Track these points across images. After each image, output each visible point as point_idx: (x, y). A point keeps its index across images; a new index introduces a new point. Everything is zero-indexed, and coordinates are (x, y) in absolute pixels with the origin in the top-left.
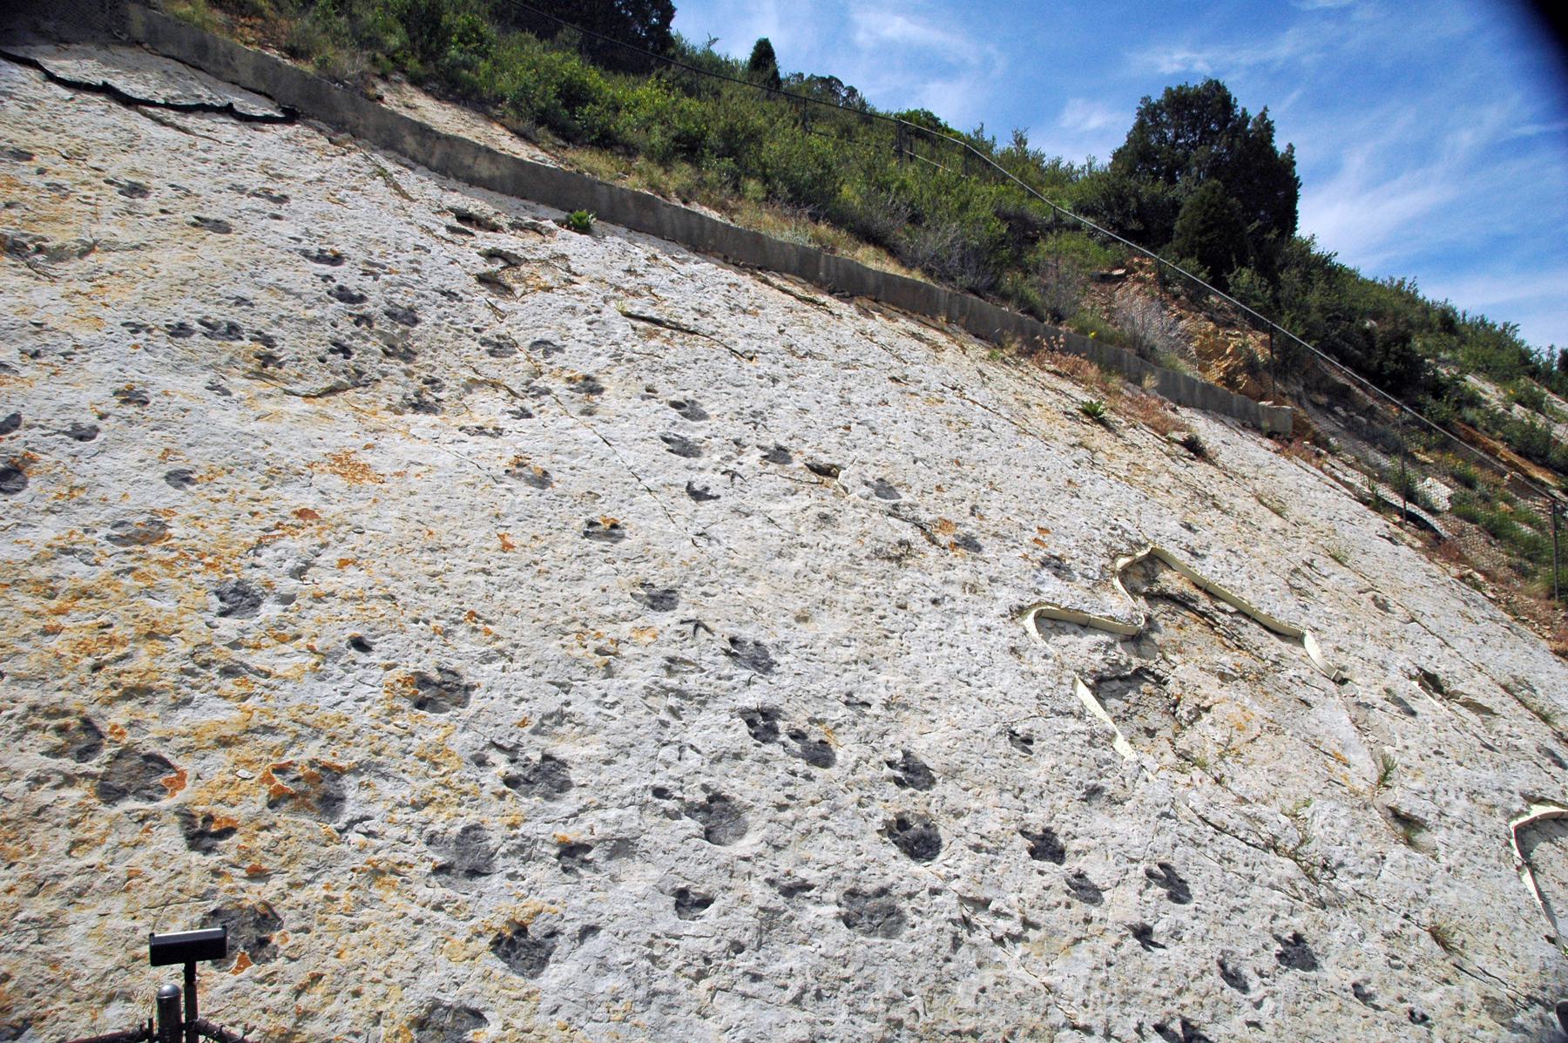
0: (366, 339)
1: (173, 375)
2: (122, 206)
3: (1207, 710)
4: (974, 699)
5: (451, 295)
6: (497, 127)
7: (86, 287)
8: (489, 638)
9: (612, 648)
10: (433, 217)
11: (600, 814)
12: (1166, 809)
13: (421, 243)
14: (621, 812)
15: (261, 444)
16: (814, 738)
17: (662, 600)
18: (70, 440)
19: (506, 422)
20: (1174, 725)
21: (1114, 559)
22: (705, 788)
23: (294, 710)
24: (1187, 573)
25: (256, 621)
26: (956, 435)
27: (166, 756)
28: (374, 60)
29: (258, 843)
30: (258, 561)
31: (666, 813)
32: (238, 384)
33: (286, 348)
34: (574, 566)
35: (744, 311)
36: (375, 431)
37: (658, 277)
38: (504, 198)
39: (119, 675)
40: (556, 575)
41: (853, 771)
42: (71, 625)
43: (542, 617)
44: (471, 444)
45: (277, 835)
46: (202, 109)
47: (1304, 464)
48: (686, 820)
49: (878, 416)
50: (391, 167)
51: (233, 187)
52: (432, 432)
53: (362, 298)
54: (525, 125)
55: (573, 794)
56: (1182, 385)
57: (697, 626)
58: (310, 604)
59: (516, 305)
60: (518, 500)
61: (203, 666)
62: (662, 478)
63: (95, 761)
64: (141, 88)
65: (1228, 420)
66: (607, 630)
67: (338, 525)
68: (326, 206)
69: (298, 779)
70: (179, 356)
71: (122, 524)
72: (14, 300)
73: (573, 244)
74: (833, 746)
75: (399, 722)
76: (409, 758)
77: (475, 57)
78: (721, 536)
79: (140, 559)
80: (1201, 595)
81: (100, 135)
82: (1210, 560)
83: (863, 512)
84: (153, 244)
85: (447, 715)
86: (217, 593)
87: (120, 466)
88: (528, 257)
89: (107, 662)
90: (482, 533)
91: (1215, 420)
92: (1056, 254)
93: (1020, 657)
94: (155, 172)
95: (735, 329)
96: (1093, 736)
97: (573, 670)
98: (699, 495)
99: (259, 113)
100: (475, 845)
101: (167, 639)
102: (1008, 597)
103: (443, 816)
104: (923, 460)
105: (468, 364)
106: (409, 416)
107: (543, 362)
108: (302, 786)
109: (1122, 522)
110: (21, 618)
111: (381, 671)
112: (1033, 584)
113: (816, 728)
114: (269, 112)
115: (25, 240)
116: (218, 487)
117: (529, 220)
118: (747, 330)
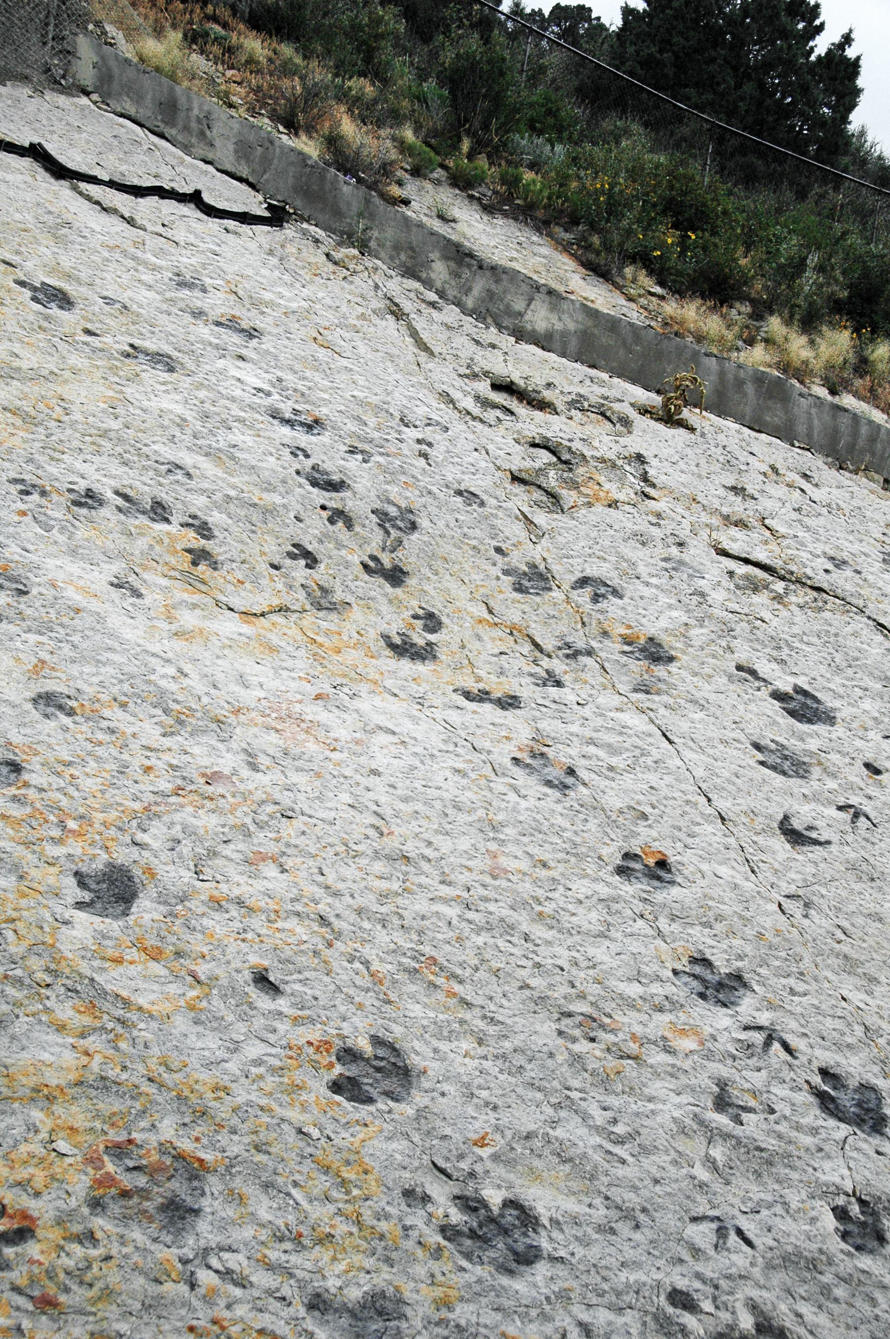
5: (469, 496)
9: (633, 1048)
10: (459, 382)
14: (611, 1316)
15: (171, 671)
22: (753, 1307)
30: (140, 837)
43: (533, 982)
55: (542, 1269)
86: (76, 874)
90: (464, 844)
108: (142, 1181)
116: (104, 724)
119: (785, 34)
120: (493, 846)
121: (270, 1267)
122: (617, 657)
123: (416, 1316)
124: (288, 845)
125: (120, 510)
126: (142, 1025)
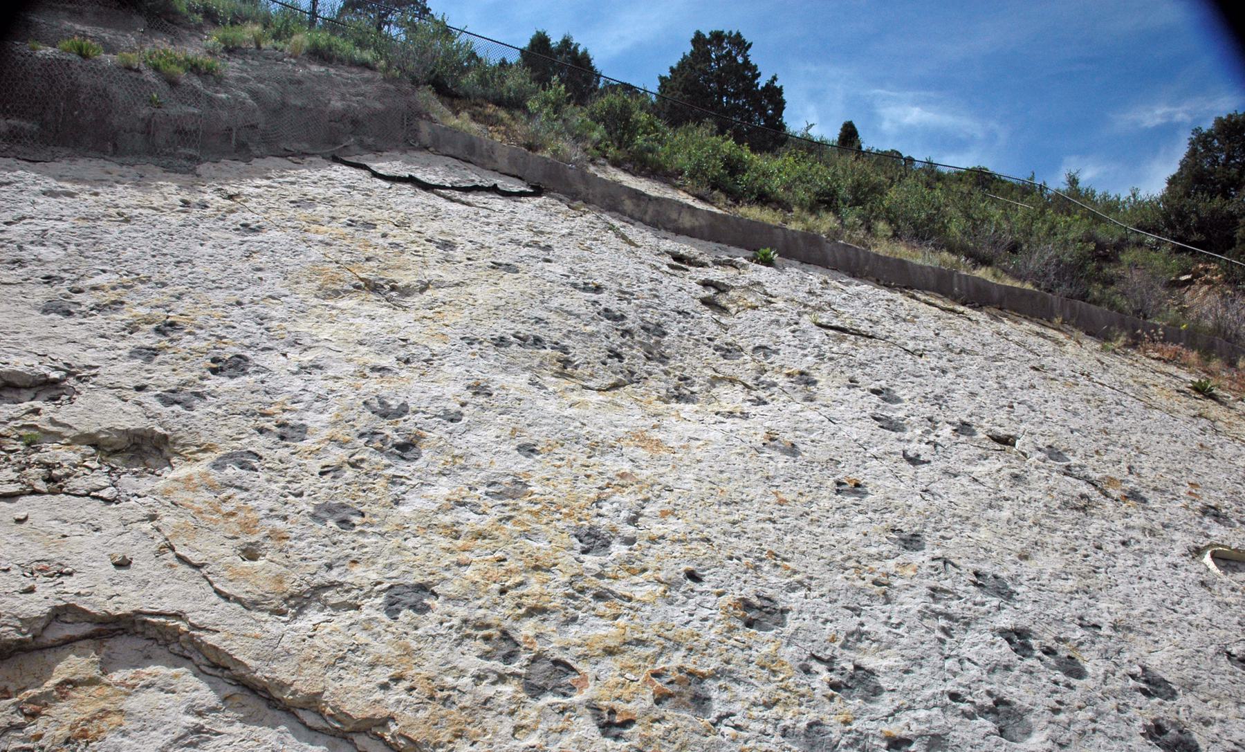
0: (631, 348)
1: (504, 375)
2: (441, 256)
6: (681, 193)
7: (430, 314)
8: (788, 572)
9: (884, 579)
10: (658, 258)
11: (912, 714)
13: (654, 276)
14: (928, 712)
15: (578, 424)
16: (1065, 655)
17: (912, 542)
18: (445, 422)
19: (747, 407)
22: (989, 693)
25: (610, 558)
26: (1096, 411)
27: (569, 661)
28: (585, 150)
29: (654, 733)
30: (601, 511)
31: (964, 714)
32: (549, 380)
33: (577, 355)
34: (837, 516)
35: (904, 320)
36: (655, 415)
37: (832, 296)
38: (703, 242)
39: (520, 597)
40: (826, 523)
41: (1105, 682)
42: (477, 559)
43: (824, 555)
44: (729, 424)
46: (476, 189)
48: (982, 720)
49: (1033, 397)
50: (617, 224)
51: (512, 241)
53: (623, 317)
54: (703, 190)
55: (886, 697)
57: (945, 563)
58: (648, 545)
59: (735, 320)
60: (780, 465)
61: (580, 592)
63: (517, 664)
64: (434, 177)
66: (875, 565)
67: (652, 485)
68: (578, 252)
69: (671, 682)
70: (505, 360)
71: (494, 483)
73: (764, 274)
75: (739, 638)
76: (753, 667)
77: (656, 144)
78: (941, 492)
79: (514, 510)
81: (415, 210)
83: (1045, 473)
84: (468, 281)
85: (773, 632)
88: (734, 285)
89: (509, 587)
90: (761, 491)
94: (457, 232)
95: (903, 332)
98: (915, 461)
99: (516, 190)
100: (819, 738)
101: (548, 571)
103: (790, 714)
104: (1078, 430)
105: (708, 365)
106: (674, 405)
107: (765, 362)
108: (676, 688)
110: (441, 553)
111: (715, 598)
113: (1062, 646)
114: (523, 189)
115: (382, 282)
116: (557, 456)
117: (726, 258)
118: (911, 334)
119: (745, 78)
120: (774, 489)
121: (756, 720)
122: (790, 384)
124: (676, 505)
126: (643, 609)
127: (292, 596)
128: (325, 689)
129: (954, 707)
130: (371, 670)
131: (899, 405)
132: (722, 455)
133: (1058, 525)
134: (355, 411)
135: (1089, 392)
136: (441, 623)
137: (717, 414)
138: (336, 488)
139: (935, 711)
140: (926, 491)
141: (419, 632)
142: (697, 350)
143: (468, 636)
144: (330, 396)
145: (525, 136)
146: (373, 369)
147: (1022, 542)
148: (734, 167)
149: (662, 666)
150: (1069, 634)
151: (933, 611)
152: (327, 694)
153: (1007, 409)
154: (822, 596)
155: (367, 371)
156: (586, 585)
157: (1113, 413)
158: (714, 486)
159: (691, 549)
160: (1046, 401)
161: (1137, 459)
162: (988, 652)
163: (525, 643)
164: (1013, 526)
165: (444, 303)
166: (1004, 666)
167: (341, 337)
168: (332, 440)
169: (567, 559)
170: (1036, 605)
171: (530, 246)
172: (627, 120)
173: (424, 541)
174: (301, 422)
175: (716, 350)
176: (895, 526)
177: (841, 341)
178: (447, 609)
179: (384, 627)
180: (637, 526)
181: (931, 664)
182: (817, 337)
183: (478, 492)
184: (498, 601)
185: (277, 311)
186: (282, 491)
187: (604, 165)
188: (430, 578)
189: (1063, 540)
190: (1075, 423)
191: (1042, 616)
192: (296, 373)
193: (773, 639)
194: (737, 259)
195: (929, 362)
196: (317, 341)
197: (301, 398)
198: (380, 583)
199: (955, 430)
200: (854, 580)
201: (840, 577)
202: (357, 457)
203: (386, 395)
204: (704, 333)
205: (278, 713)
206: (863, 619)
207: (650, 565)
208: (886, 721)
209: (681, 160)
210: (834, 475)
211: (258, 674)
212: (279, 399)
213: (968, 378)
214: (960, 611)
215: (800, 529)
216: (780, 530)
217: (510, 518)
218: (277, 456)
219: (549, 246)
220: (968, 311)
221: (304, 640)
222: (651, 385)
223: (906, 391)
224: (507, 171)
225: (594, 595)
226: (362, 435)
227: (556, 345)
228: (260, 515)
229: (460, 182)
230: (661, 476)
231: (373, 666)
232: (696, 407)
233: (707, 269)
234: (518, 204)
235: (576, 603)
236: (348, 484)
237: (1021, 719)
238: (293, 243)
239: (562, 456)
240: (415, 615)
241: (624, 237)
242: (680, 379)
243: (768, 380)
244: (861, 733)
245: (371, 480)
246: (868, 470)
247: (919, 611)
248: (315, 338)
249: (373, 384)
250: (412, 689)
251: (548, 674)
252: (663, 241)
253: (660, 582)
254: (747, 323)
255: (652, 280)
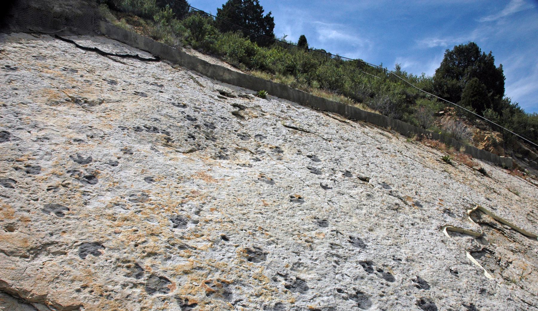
0: (199, 133)
1: (139, 144)
2: (110, 88)
3: (511, 263)
4: (435, 258)
6: (225, 63)
7: (103, 115)
8: (268, 236)
9: (310, 240)
11: (321, 298)
12: (509, 297)
13: (211, 101)
14: (328, 298)
15: (173, 168)
16: (386, 272)
17: (323, 223)
19: (251, 162)
20: (500, 268)
21: (466, 210)
22: (354, 289)
23: (207, 261)
24: (491, 215)
26: (403, 167)
27: (167, 277)
28: (181, 41)
30: (183, 208)
31: (343, 298)
32: (160, 148)
33: (174, 136)
34: (290, 211)
35: (323, 125)
36: (209, 165)
37: (292, 113)
38: (234, 86)
39: (144, 248)
40: (285, 214)
42: (124, 230)
43: (284, 229)
44: (243, 169)
45: (212, 306)
47: (519, 178)
48: (351, 300)
49: (377, 161)
50: (195, 76)
51: (144, 82)
52: (229, 166)
53: (196, 119)
54: (235, 63)
55: (310, 291)
56: (473, 151)
57: (337, 232)
58: (204, 224)
59: (247, 122)
60: (265, 189)
61: (172, 245)
62: (311, 182)
63: (142, 279)
64: (107, 49)
65: (489, 163)
66: (306, 233)
67: (207, 197)
68: (176, 88)
69: (214, 286)
70: (139, 138)
71: (133, 195)
72: (79, 119)
73: (261, 102)
74: (393, 274)
75: (245, 266)
76: (251, 279)
77: (214, 40)
78: (336, 202)
79: (142, 207)
80: (498, 223)
81: (97, 65)
82: (498, 211)
84: (123, 100)
85: (260, 263)
86: (171, 220)
87: (128, 175)
89: (139, 243)
91: (486, 163)
92: (421, 106)
93: (445, 244)
94: (118, 77)
95: (322, 130)
96: (477, 271)
97: (299, 248)
98: (325, 187)
99: (147, 58)
101: (158, 236)
102: (436, 223)
103: (267, 299)
104: (395, 176)
106: (218, 160)
107: (260, 142)
108: (216, 289)
109: (465, 197)
110: (107, 228)
111: (234, 248)
112: (443, 219)
113: (386, 268)
114: (150, 57)
115: (80, 99)
116: (163, 183)
117: (244, 94)
118: (326, 131)
119: (257, 12)
120: (262, 199)
121: (252, 302)
122: (271, 152)
123: (287, 308)
124: (217, 206)
125: (147, 131)
126: (201, 253)
127: (32, 249)
128: (48, 293)
129: (339, 295)
130: (72, 283)
131: (319, 163)
132: (240, 183)
133: (386, 216)
134: (65, 160)
135: (401, 159)
136: (106, 260)
137: (237, 165)
138: (55, 197)
139: (331, 297)
140: (330, 201)
141: (96, 265)
142: (229, 135)
143: (119, 266)
144: (53, 153)
145: (152, 32)
146: (75, 140)
147: (370, 224)
148: (250, 53)
149: (210, 279)
150: (388, 263)
151: (331, 254)
152: (49, 295)
153: (366, 166)
154: (283, 247)
155: (72, 141)
156: (175, 242)
157: (410, 169)
158: (235, 198)
159: (224, 226)
160: (383, 163)
161: (419, 189)
162: (354, 271)
163: (146, 269)
164: (367, 217)
165: (111, 110)
166: (361, 277)
167: (59, 124)
168: (53, 174)
169: (166, 230)
170: (375, 251)
171: (153, 85)
172: (201, 28)
173: (98, 222)
174: (38, 165)
175: (238, 136)
176: (316, 216)
177: (295, 134)
178: (109, 254)
179: (78, 263)
180: (200, 215)
181: (330, 276)
182: (284, 131)
183: (125, 199)
184: (134, 250)
185: (26, 110)
186: (27, 198)
187: (190, 48)
188: (101, 239)
189: (387, 223)
190: (394, 172)
191: (377, 256)
192: (36, 141)
193: (260, 266)
194: (249, 95)
195: (333, 144)
196: (47, 126)
197: (38, 153)
198: (77, 242)
199: (344, 175)
200: (297, 240)
201: (291, 238)
202: (66, 182)
203: (81, 153)
204: (233, 128)
205: (23, 305)
206: (300, 257)
207: (205, 233)
208: (310, 302)
209: (225, 48)
210: (289, 193)
211: (13, 287)
212: (26, 153)
213: (350, 152)
214: (343, 253)
215: (274, 217)
216: (264, 217)
217: (140, 211)
218: (25, 181)
219: (162, 85)
220: (351, 122)
221: (38, 270)
222: (208, 151)
223: (323, 156)
224: (143, 49)
225: (179, 247)
226: (69, 172)
227: (164, 132)
228: (16, 209)
229: (120, 52)
230: (211, 192)
231: (72, 281)
232: (228, 161)
233: (236, 99)
234: (148, 64)
235: (170, 250)
236: (61, 195)
237: (367, 300)
238: (34, 77)
239: (165, 183)
240: (94, 257)
241: (198, 82)
242: (221, 149)
243: (262, 150)
244: (299, 307)
245: (73, 193)
246: (305, 191)
247: (325, 254)
248: (46, 124)
249: (75, 148)
250: (92, 291)
251: (157, 283)
252: (216, 85)
253: (209, 241)
254: (253, 124)
255: (210, 103)
